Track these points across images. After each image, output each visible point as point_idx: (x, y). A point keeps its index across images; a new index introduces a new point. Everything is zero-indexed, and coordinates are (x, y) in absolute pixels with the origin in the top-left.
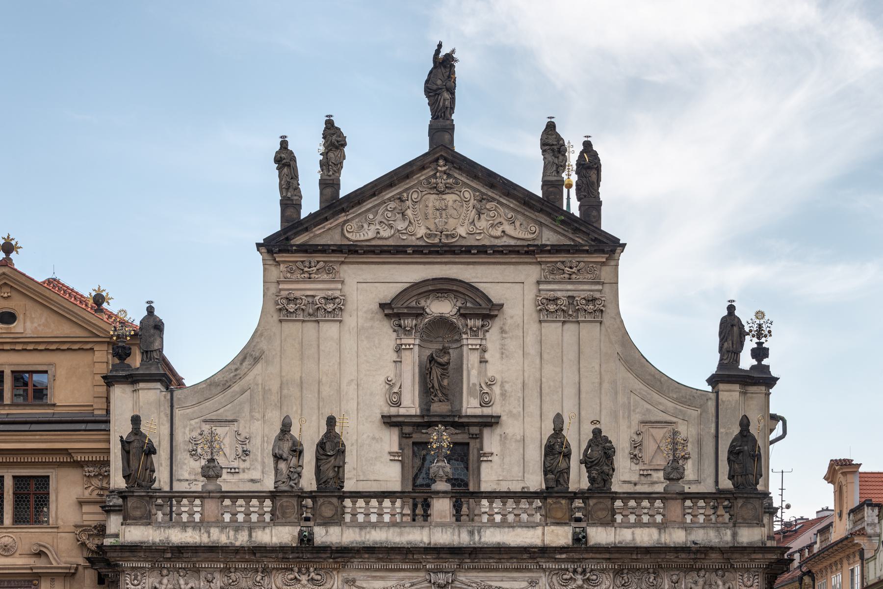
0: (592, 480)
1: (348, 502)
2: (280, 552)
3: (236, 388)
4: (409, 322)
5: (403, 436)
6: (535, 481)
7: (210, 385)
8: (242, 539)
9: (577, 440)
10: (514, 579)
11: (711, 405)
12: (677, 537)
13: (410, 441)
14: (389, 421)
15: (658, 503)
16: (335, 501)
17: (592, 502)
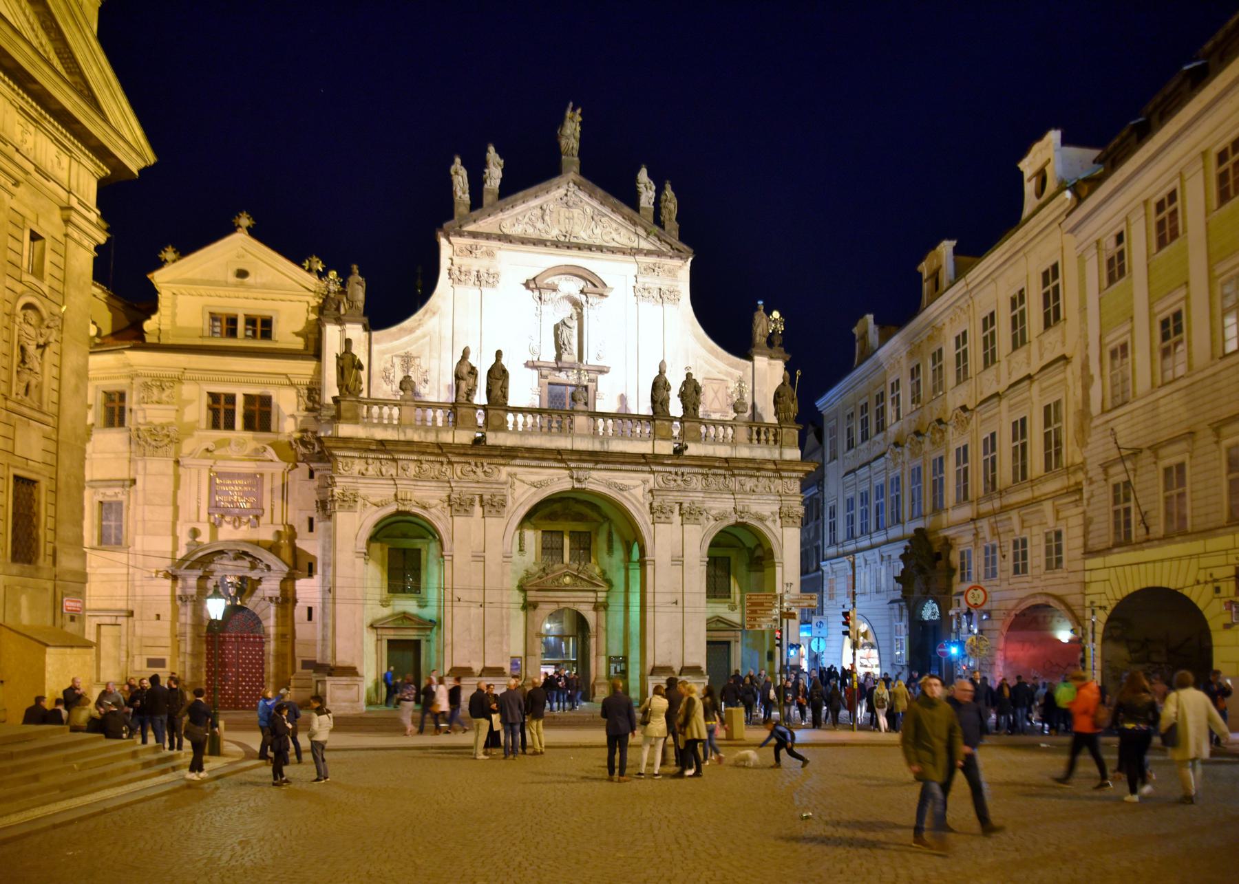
0: (685, 408)
1: (510, 417)
2: (461, 451)
3: (418, 333)
4: (547, 295)
5: (542, 376)
6: (645, 409)
7: (400, 330)
8: (431, 438)
9: (676, 381)
10: (632, 479)
11: (750, 370)
12: (744, 452)
13: (546, 381)
14: (531, 365)
15: (730, 431)
16: (501, 412)
17: (687, 424)
